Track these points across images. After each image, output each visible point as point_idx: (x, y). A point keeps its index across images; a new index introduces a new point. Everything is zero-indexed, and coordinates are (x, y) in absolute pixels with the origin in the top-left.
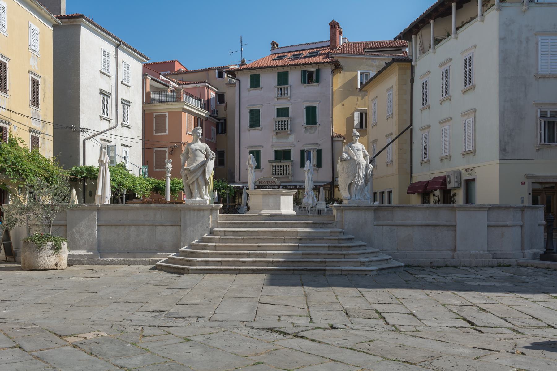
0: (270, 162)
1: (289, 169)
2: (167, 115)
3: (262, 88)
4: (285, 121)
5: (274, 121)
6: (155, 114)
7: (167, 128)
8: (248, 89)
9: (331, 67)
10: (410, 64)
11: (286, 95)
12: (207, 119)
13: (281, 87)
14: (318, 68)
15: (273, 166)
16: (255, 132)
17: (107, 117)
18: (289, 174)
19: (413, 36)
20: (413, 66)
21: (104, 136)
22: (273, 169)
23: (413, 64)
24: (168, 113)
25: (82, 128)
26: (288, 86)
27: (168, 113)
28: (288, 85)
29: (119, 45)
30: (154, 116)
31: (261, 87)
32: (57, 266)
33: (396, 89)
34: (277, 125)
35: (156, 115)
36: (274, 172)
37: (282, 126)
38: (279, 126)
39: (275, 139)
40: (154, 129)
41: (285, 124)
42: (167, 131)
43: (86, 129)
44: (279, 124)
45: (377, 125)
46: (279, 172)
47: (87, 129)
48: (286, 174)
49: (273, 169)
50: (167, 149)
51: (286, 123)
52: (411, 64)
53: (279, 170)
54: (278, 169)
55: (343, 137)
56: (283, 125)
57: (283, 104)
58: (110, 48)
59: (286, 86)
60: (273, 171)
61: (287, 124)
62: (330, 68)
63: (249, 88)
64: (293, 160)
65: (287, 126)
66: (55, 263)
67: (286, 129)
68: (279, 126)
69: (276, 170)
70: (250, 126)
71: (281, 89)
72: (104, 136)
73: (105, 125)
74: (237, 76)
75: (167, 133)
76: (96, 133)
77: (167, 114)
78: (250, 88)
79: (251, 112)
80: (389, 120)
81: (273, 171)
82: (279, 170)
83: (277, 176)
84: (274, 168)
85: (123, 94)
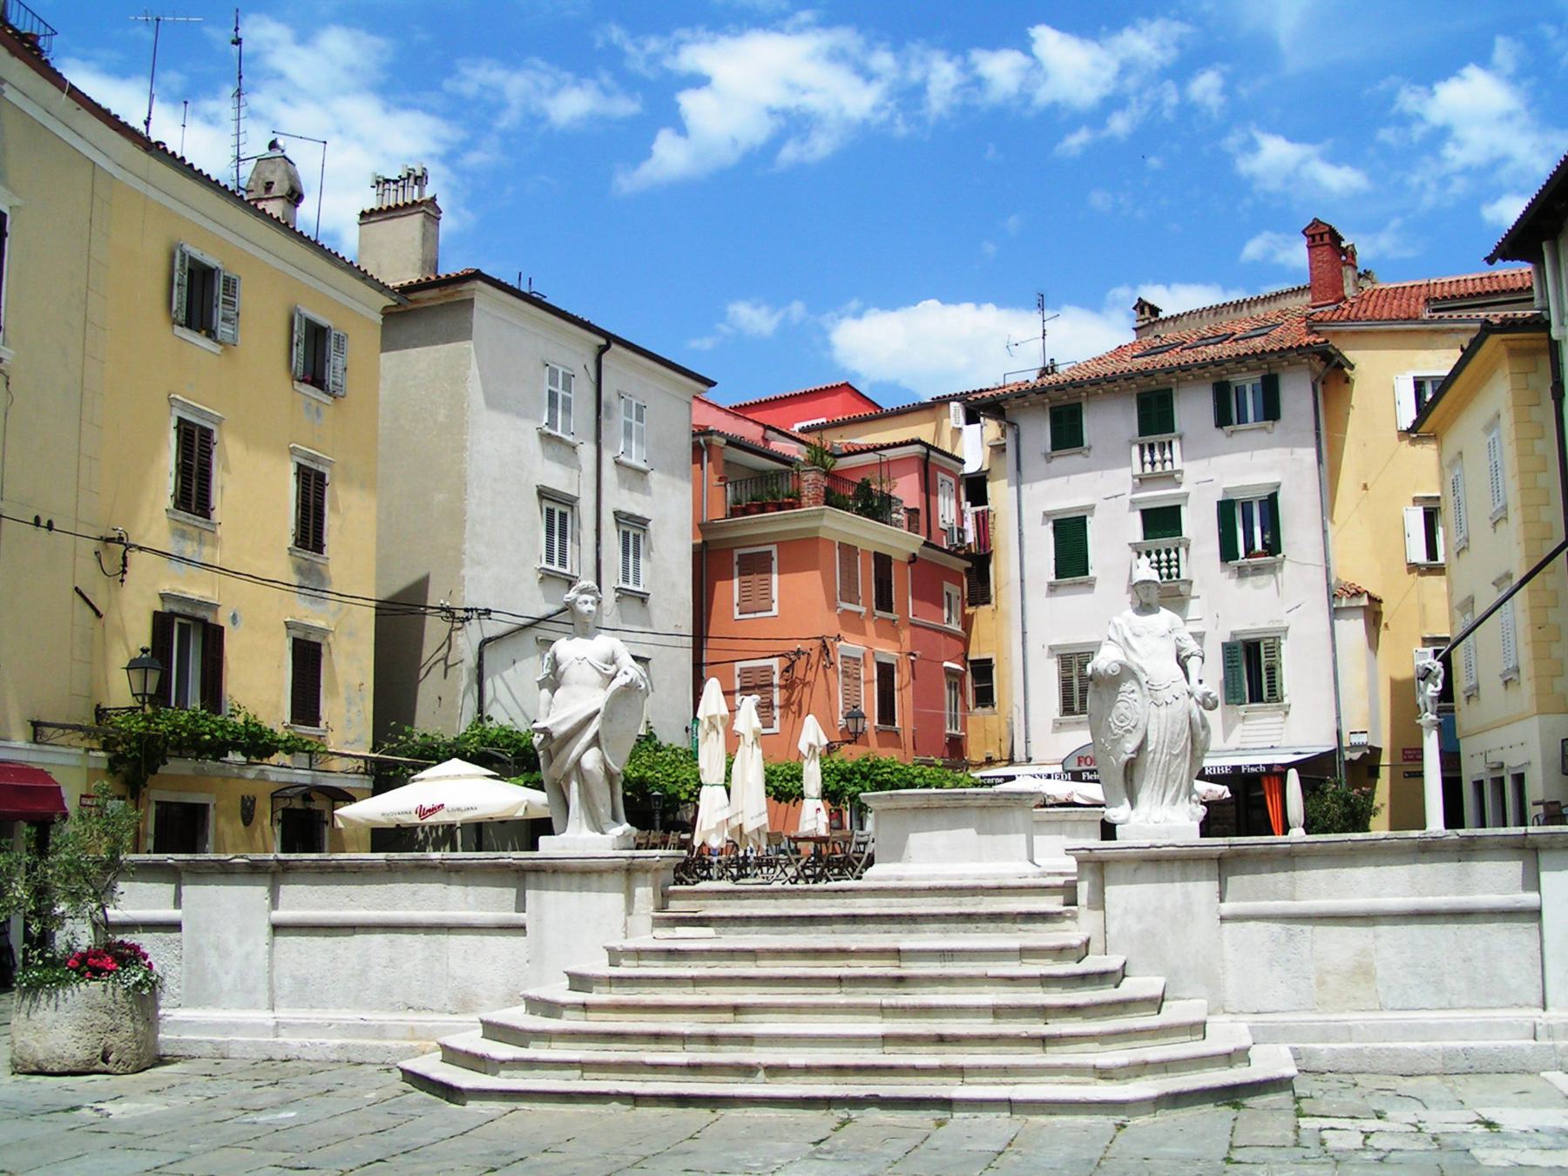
2: (775, 555)
3: (1089, 449)
4: (1168, 552)
6: (737, 552)
7: (775, 595)
8: (1046, 455)
9: (1310, 364)
10: (1545, 335)
11: (1168, 464)
12: (913, 559)
13: (1151, 441)
14: (1266, 373)
17: (562, 570)
19: (1545, 246)
20: (1556, 342)
23: (1555, 334)
24: (775, 546)
25: (472, 610)
26: (1173, 434)
27: (775, 546)
28: (1173, 431)
30: (736, 559)
31: (1086, 444)
32: (105, 1059)
33: (1507, 420)
35: (740, 556)
40: (736, 600)
42: (775, 606)
43: (486, 610)
45: (1468, 548)
47: (488, 612)
50: (775, 663)
51: (1173, 555)
52: (1550, 335)
55: (1366, 595)
57: (1159, 496)
59: (1165, 437)
61: (1177, 560)
62: (1307, 366)
63: (1049, 450)
65: (1178, 567)
66: (99, 1051)
70: (1056, 573)
71: (1151, 447)
74: (1006, 412)
75: (775, 612)
76: (522, 621)
77: (774, 549)
78: (1053, 450)
80: (1499, 527)
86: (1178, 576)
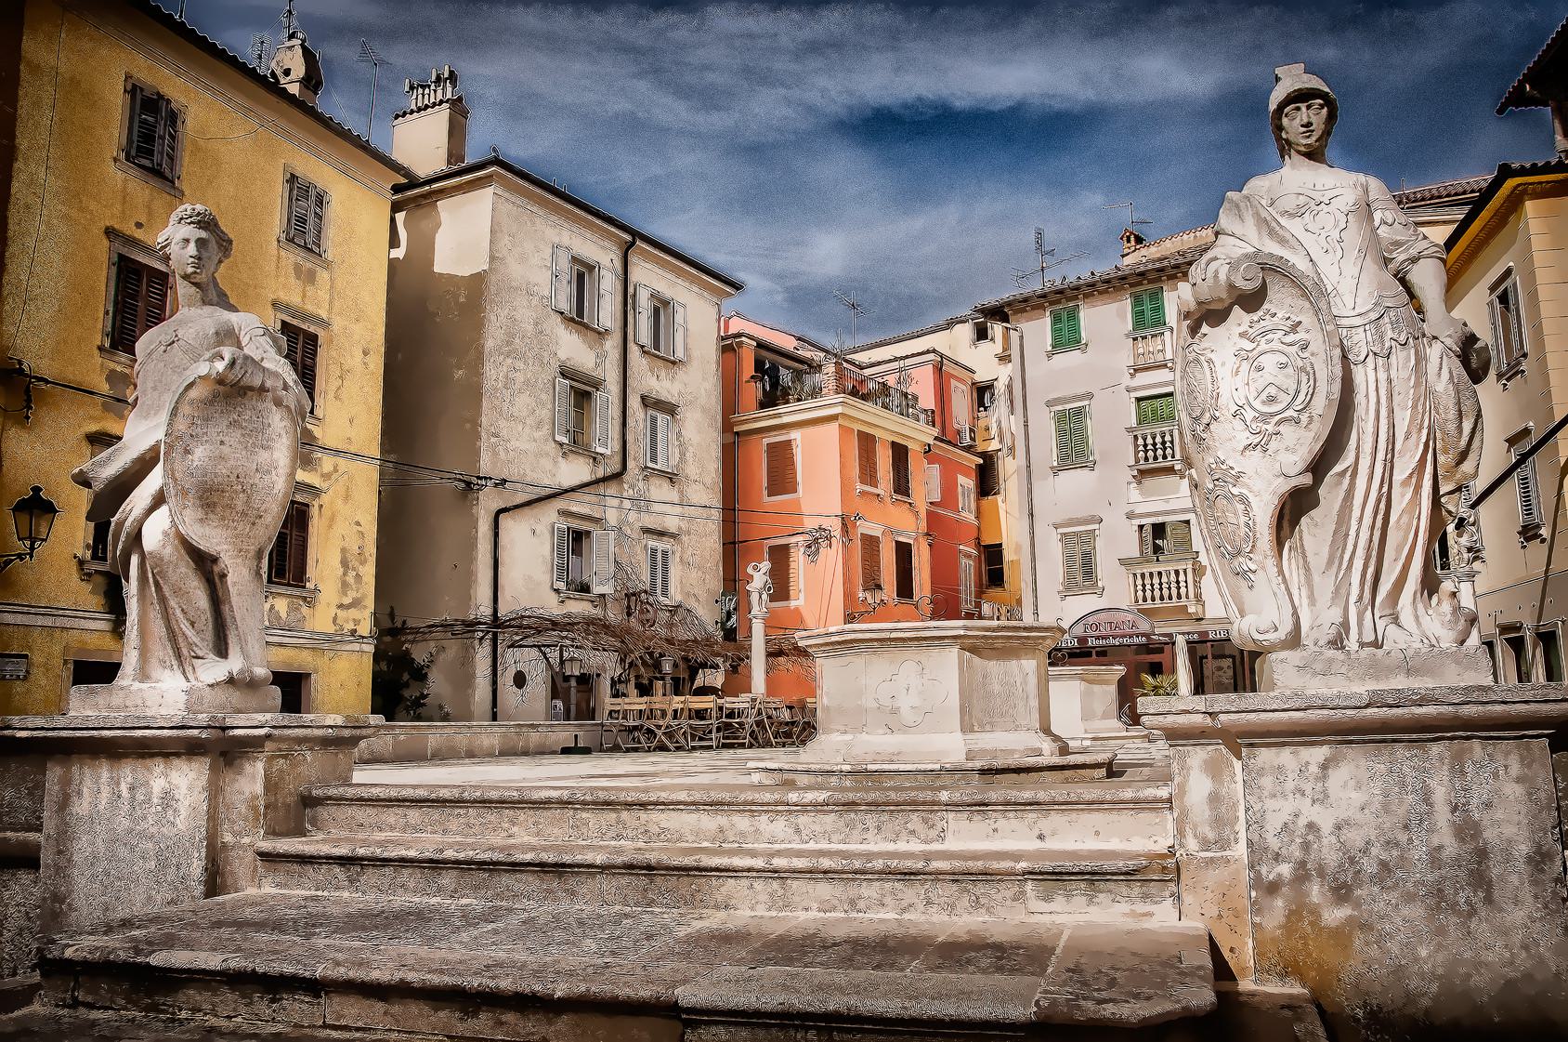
0: (1123, 562)
1: (1186, 582)
5: (1131, 439)
15: (1135, 575)
16: (1075, 480)
18: (1187, 597)
21: (578, 505)
22: (1136, 586)
29: (633, 244)
34: (1141, 448)
36: (1140, 594)
37: (1155, 450)
38: (1146, 451)
39: (1134, 493)
41: (1164, 443)
44: (1145, 445)
46: (1157, 593)
48: (1179, 596)
49: (1136, 586)
53: (1157, 586)
54: (1152, 585)
56: (1159, 446)
58: (602, 253)
60: (1136, 591)
61: (1172, 442)
64: (1197, 552)
67: (1169, 458)
68: (1146, 451)
69: (1144, 585)
72: (578, 505)
73: (575, 471)
79: (1061, 418)
81: (1136, 591)
82: (1157, 586)
83: (1149, 604)
84: (1139, 582)
85: (648, 379)
86: (1173, 456)
